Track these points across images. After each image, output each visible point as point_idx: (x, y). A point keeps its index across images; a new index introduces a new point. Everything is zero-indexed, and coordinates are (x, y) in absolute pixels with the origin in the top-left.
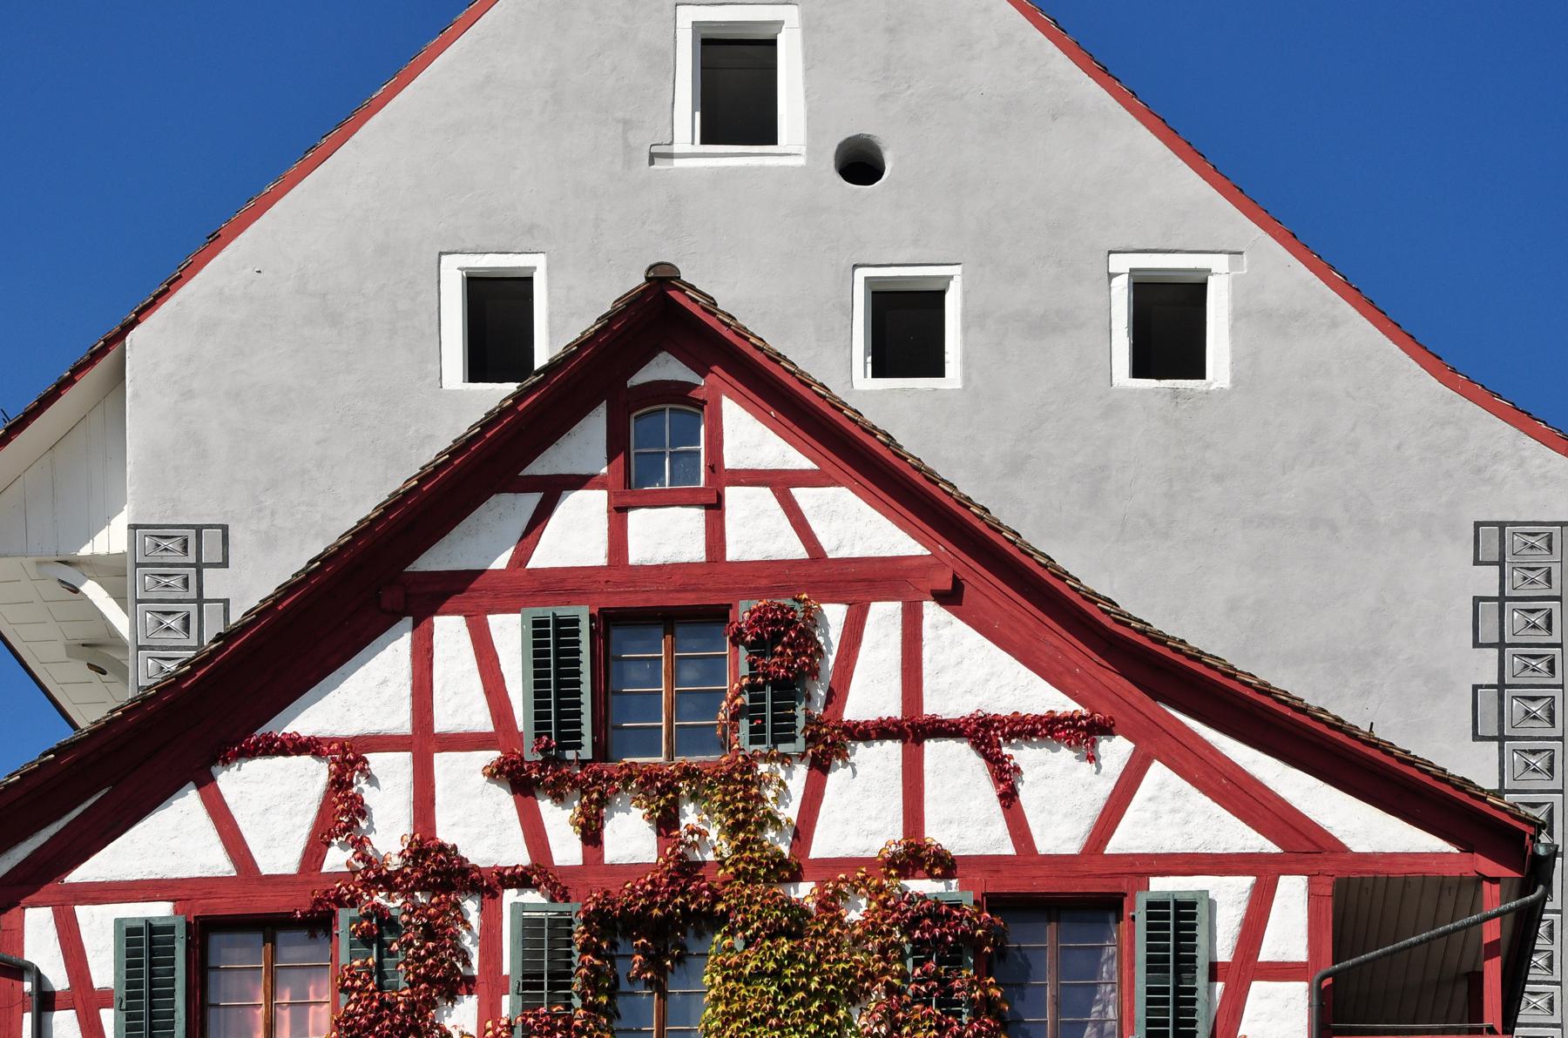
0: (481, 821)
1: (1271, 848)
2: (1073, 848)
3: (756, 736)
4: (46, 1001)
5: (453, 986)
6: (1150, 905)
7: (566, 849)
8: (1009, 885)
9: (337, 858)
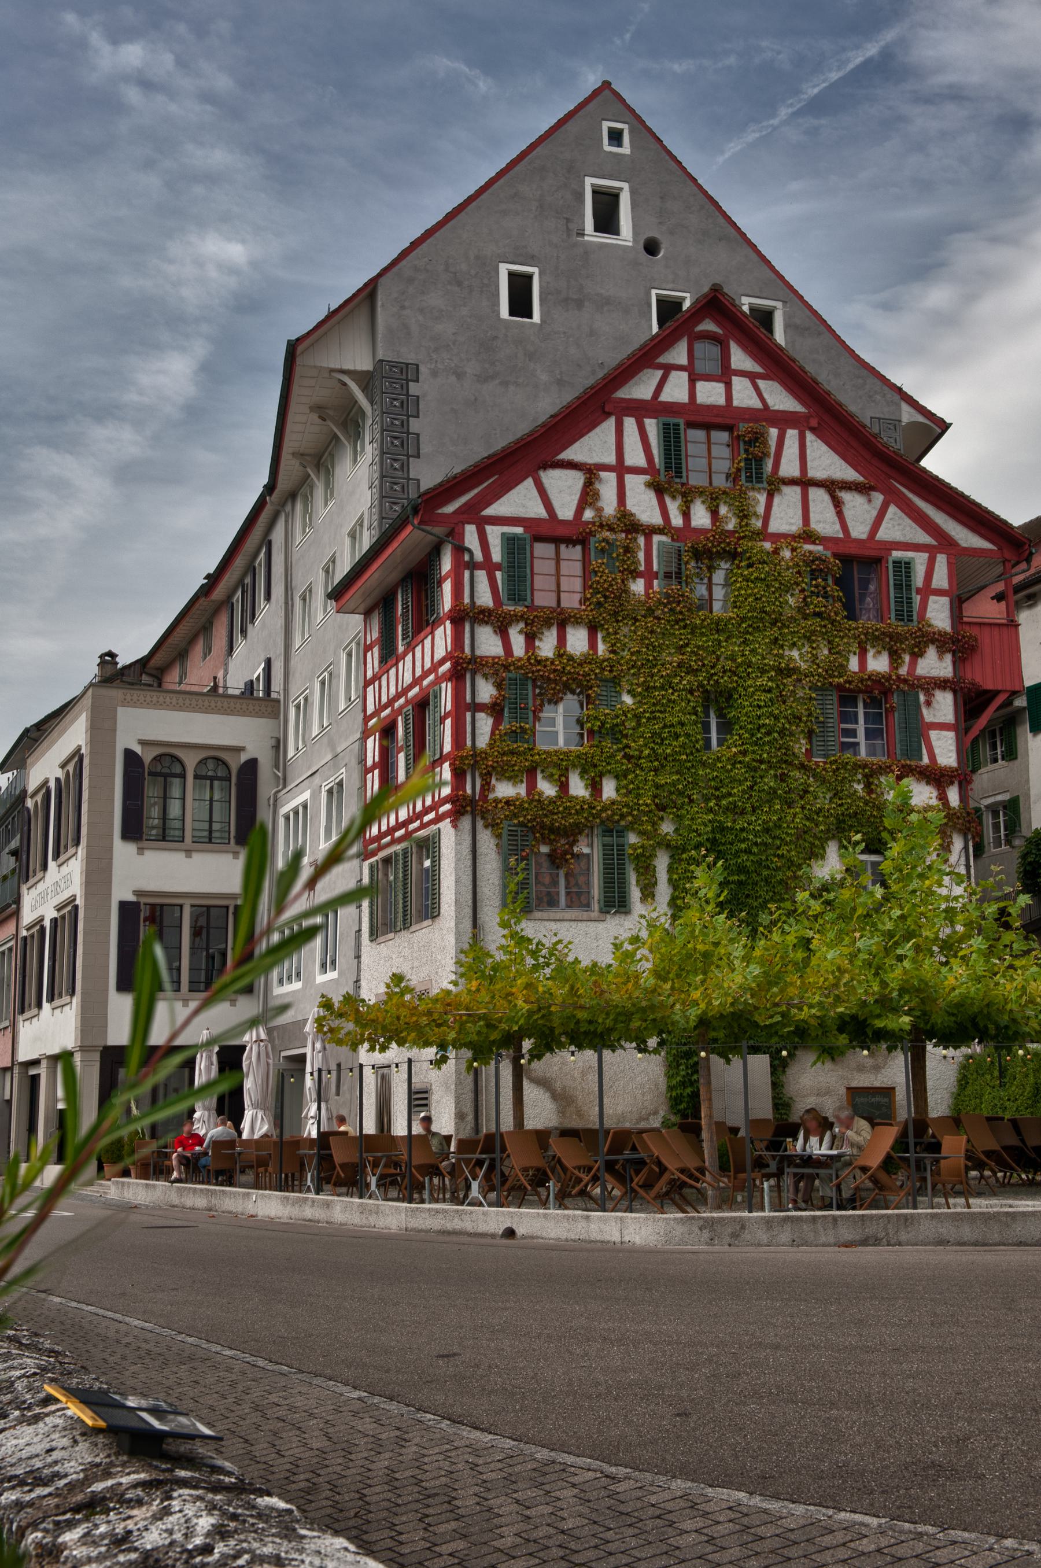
0: (644, 505)
1: (934, 543)
2: (864, 537)
3: (749, 479)
4: (473, 566)
5: (635, 574)
6: (894, 562)
7: (677, 521)
8: (841, 550)
9: (588, 515)
